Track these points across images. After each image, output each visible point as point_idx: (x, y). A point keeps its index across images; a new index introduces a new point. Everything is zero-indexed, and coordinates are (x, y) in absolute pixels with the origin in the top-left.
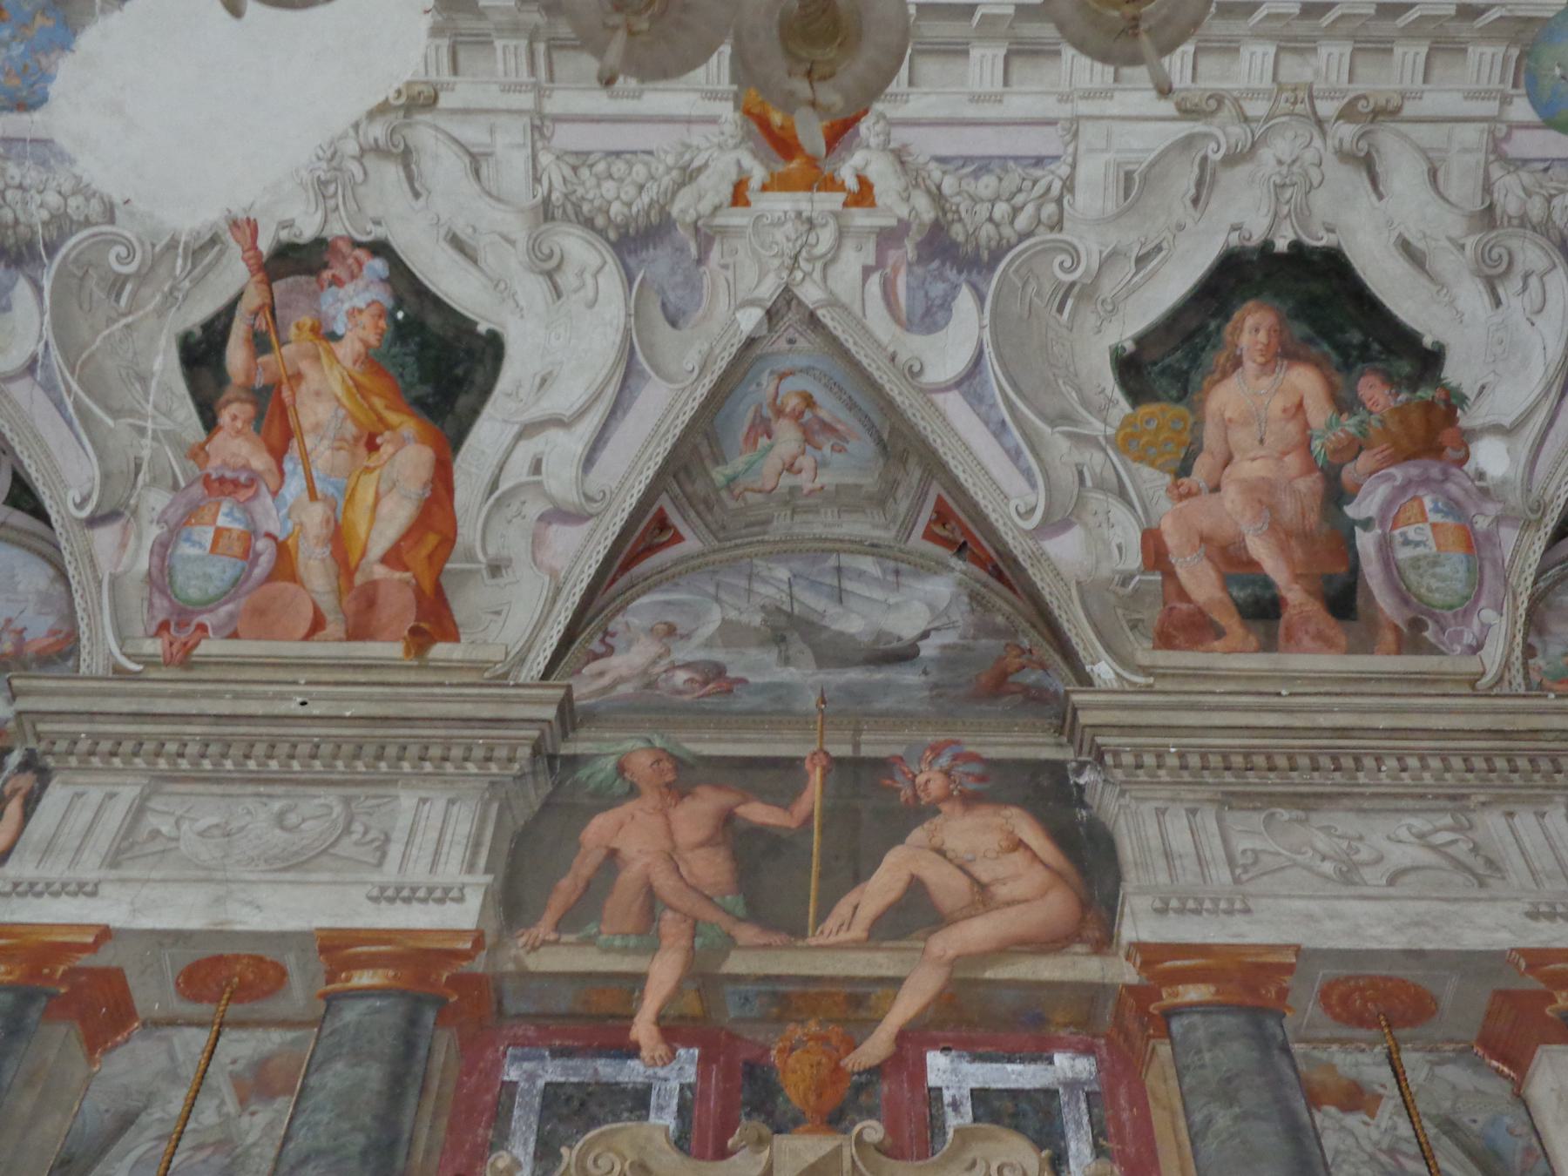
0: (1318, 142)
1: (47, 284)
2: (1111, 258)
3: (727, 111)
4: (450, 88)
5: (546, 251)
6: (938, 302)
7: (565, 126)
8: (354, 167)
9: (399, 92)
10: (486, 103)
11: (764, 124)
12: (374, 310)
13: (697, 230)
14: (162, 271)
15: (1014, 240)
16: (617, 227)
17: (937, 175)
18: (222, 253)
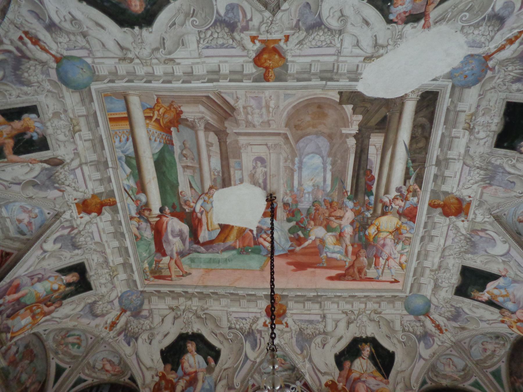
0: (137, 53)
1: (490, 9)
2: (183, 24)
3: (289, 58)
4: (360, 62)
5: (342, 22)
6: (230, 12)
7: (332, 53)
8: (390, 42)
9: (373, 61)
10: (351, 58)
11: (280, 55)
12: (396, 5)
13: (299, 29)
14: (455, 13)
15: (211, 28)
16: (321, 29)
17: (234, 44)
18: (435, 19)
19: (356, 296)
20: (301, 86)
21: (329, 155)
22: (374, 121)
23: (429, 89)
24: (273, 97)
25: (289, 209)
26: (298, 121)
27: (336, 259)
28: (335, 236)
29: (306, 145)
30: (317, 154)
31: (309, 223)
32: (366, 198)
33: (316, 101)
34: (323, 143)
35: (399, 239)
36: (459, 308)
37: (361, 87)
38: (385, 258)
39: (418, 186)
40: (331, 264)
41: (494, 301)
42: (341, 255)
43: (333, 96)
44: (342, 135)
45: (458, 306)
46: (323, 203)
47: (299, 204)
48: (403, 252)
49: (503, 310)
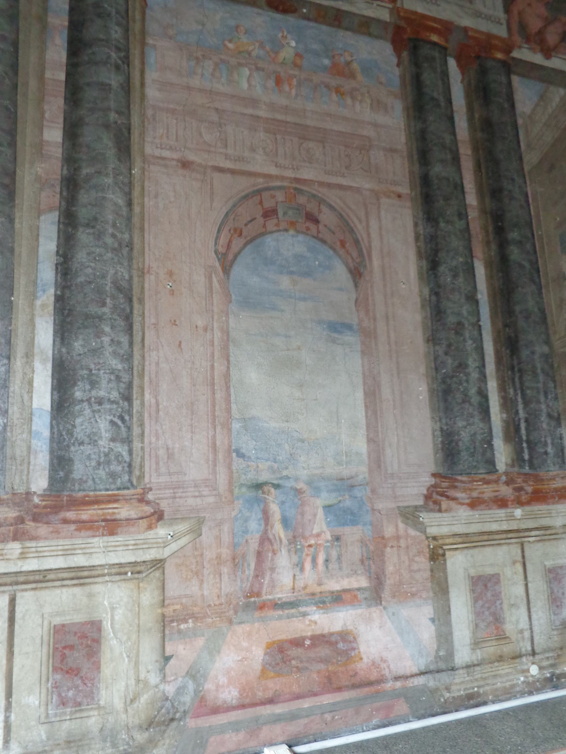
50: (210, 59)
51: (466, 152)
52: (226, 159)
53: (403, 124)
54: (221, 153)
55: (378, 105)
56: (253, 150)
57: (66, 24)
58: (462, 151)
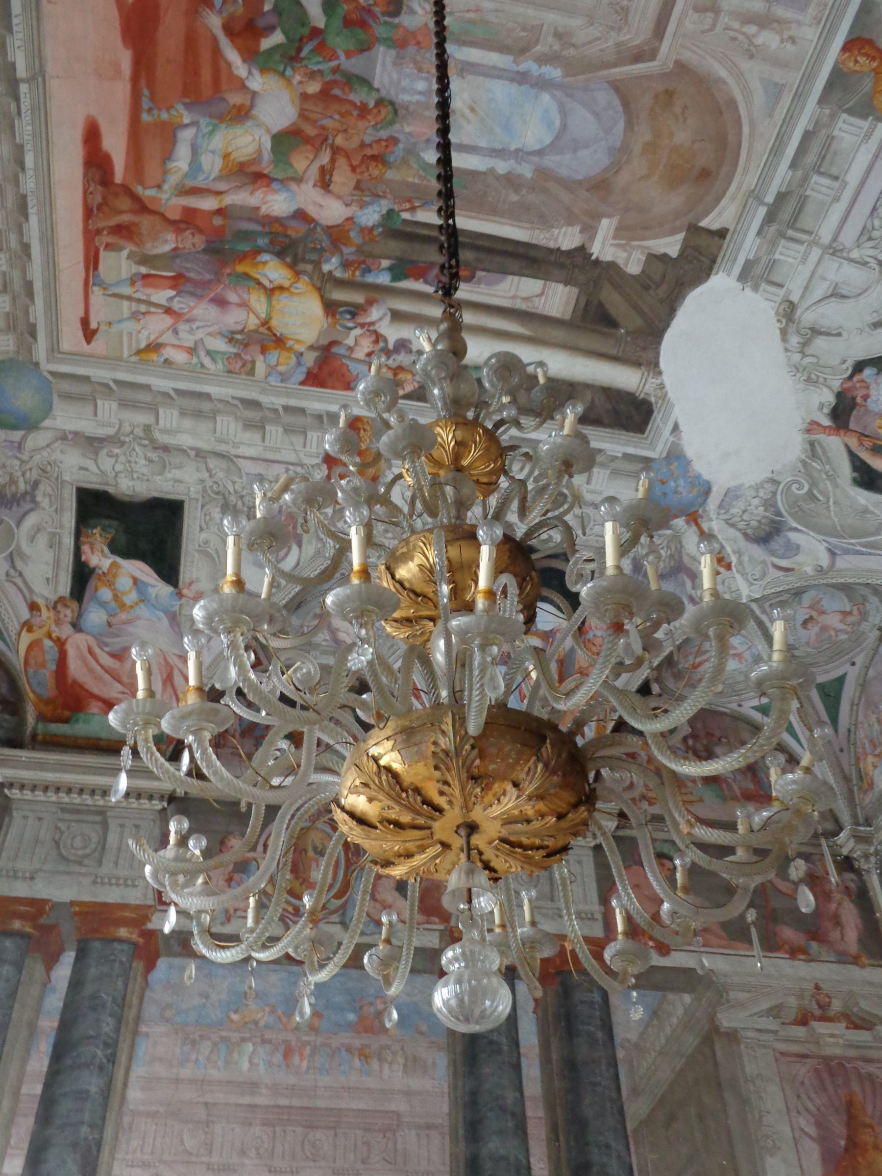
1: (795, 525)
4: (789, 292)
7: (842, 234)
8: (807, 360)
9: (779, 321)
10: (807, 276)
14: (815, 474)
18: (820, 444)
19: (26, 217)
20: (790, 138)
21: (543, 173)
22: (612, 300)
23: (657, 419)
24: (789, 47)
25: (377, 10)
26: (685, 107)
27: (168, 155)
28: (257, 158)
29: (596, 115)
30: (557, 138)
31: (312, 75)
32: (385, 263)
33: (725, 169)
34: (588, 162)
35: (246, 345)
36: (33, 500)
37: (721, 283)
38: (176, 305)
39: (412, 392)
40: (150, 139)
41: (92, 583)
42: (186, 175)
43: (720, 214)
44: (597, 217)
45: (39, 498)
46: (384, 134)
47: (393, 52)
48: (202, 353)
49: (75, 605)
50: (209, 1038)
51: (536, 1114)
52: (209, 1169)
53: (446, 1085)
54: (202, 1163)
55: (414, 1065)
56: (243, 1153)
57: (56, 1024)
58: (530, 1112)
